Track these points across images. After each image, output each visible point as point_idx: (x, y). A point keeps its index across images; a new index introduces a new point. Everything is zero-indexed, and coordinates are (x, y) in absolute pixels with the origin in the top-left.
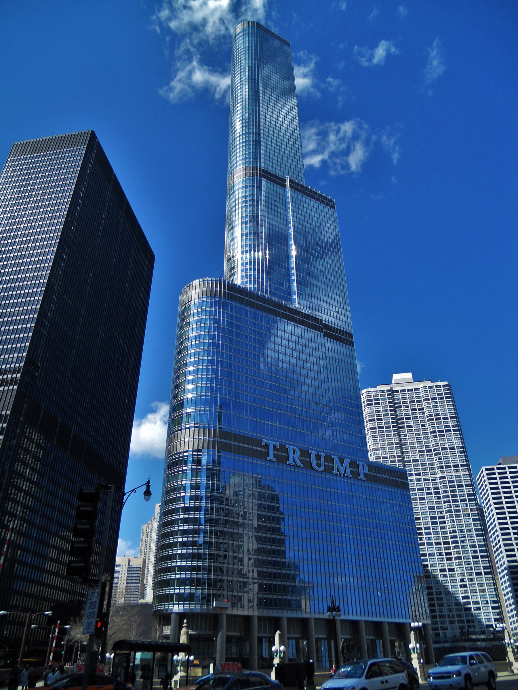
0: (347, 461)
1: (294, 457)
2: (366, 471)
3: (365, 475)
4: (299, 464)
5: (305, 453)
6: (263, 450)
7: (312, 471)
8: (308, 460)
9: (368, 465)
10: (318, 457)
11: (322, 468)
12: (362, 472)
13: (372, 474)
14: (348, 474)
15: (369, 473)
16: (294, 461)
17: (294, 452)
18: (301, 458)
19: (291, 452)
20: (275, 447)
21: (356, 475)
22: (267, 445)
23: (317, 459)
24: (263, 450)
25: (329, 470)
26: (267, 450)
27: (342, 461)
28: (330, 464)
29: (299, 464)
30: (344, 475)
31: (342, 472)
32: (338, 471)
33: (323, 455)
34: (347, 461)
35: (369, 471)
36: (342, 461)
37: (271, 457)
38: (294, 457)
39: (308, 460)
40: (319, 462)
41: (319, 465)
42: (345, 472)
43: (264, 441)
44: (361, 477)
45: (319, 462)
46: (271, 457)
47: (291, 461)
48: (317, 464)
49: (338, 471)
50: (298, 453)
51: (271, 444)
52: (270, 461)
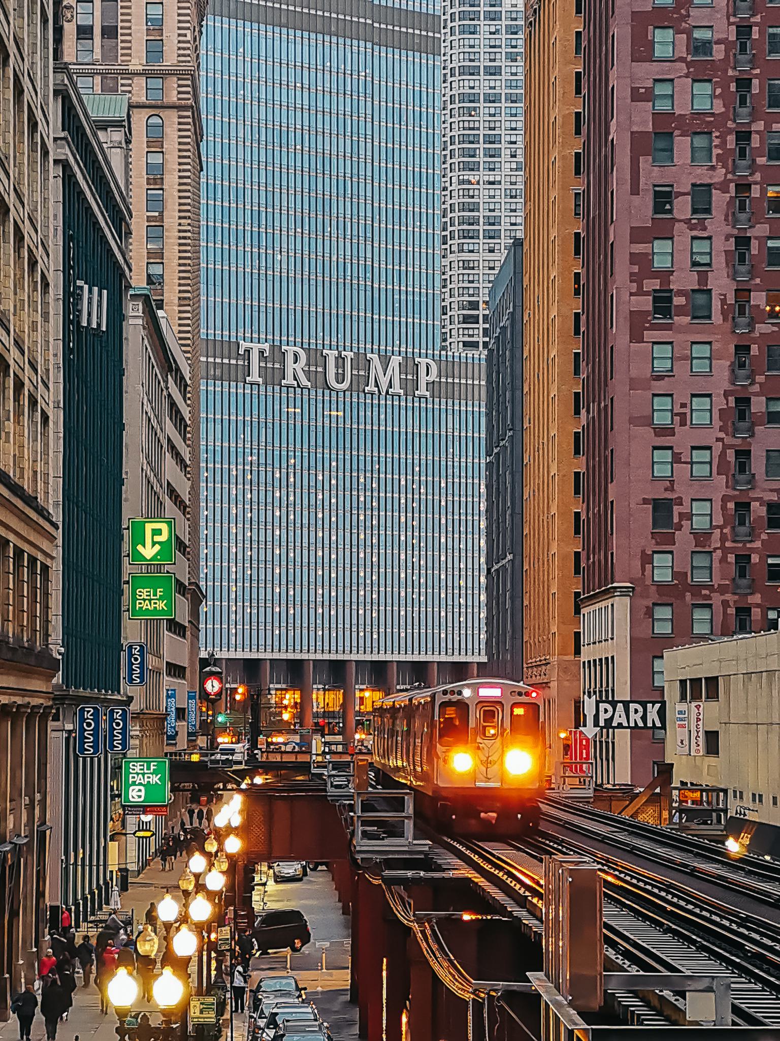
0: (396, 360)
1: (295, 369)
4: (305, 382)
5: (316, 357)
11: (345, 385)
12: (423, 380)
14: (397, 389)
19: (290, 358)
20: (261, 352)
21: (410, 386)
22: (248, 351)
23: (337, 367)
25: (359, 384)
29: (305, 382)
32: (377, 385)
33: (350, 355)
34: (396, 360)
37: (255, 377)
38: (295, 369)
43: (244, 345)
44: (422, 391)
46: (255, 377)
47: (289, 380)
49: (377, 385)
51: (256, 347)
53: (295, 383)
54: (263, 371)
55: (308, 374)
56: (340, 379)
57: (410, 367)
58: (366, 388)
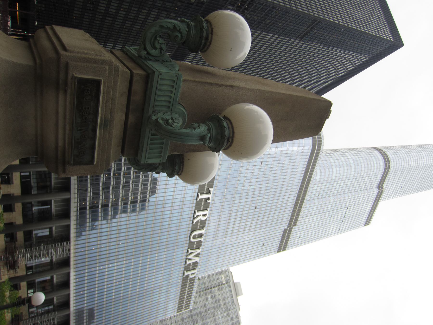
0: (197, 259)
2: (191, 276)
3: (188, 276)
4: (196, 221)
5: (203, 224)
6: (205, 190)
7: (190, 232)
8: (198, 227)
9: (195, 277)
10: (201, 236)
11: (192, 240)
13: (188, 281)
14: (188, 262)
15: (189, 278)
16: (198, 216)
17: (204, 215)
18: (199, 221)
20: (208, 199)
21: (187, 268)
22: (209, 192)
24: (205, 190)
25: (191, 246)
27: (198, 255)
28: (195, 246)
29: (196, 221)
30: (187, 259)
31: (190, 257)
32: (191, 253)
34: (197, 259)
35: (191, 278)
36: (198, 255)
37: (201, 197)
38: (200, 215)
39: (198, 227)
40: (197, 236)
41: (194, 238)
42: (190, 259)
44: (186, 273)
45: (197, 236)
46: (201, 197)
47: (197, 214)
48: (195, 235)
49: (191, 253)
50: (203, 218)
54: (201, 200)
55: (198, 222)
56: (194, 238)
57: (195, 264)
58: (189, 250)
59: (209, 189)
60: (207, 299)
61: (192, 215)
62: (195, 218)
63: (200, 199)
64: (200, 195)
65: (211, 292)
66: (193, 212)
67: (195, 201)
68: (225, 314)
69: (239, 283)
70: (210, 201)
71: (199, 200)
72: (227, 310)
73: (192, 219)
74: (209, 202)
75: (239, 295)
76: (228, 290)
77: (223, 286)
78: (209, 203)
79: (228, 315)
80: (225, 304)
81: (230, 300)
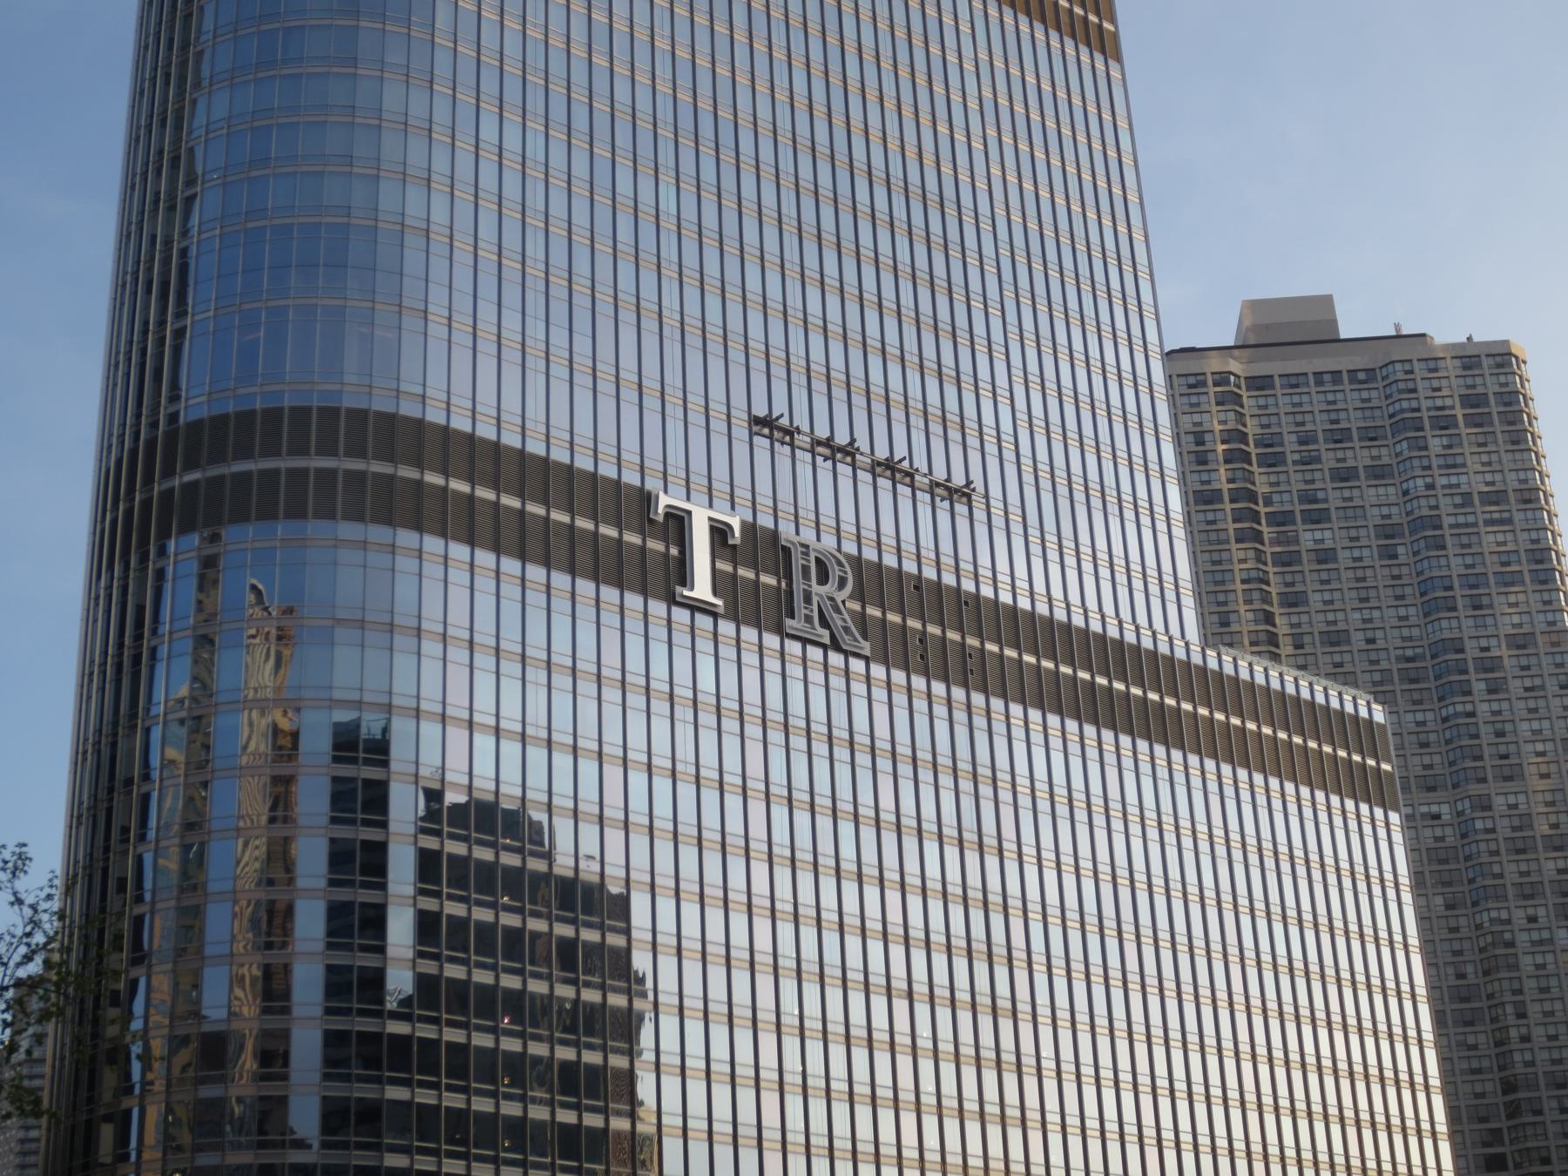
6: (655, 545)
20: (719, 533)
26: (674, 551)
37: (702, 588)
43: (664, 501)
46: (702, 588)
52: (696, 607)
53: (826, 633)
59: (651, 521)
60: (1325, 556)
61: (815, 653)
62: (833, 636)
63: (715, 593)
64: (686, 593)
65: (1281, 519)
66: (794, 648)
67: (727, 628)
68: (1436, 444)
69: (1254, 307)
70: (735, 523)
71: (719, 602)
72: (1407, 425)
73: (836, 659)
74: (737, 533)
75: (1333, 323)
76: (1283, 401)
77: (1252, 428)
78: (744, 524)
79: (1444, 423)
80: (1371, 436)
81: (1350, 397)
